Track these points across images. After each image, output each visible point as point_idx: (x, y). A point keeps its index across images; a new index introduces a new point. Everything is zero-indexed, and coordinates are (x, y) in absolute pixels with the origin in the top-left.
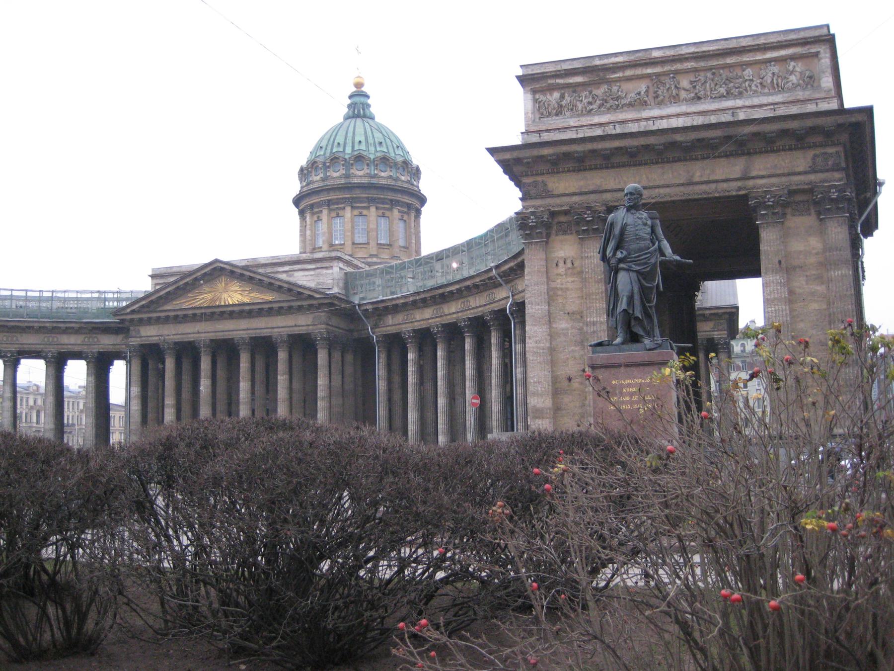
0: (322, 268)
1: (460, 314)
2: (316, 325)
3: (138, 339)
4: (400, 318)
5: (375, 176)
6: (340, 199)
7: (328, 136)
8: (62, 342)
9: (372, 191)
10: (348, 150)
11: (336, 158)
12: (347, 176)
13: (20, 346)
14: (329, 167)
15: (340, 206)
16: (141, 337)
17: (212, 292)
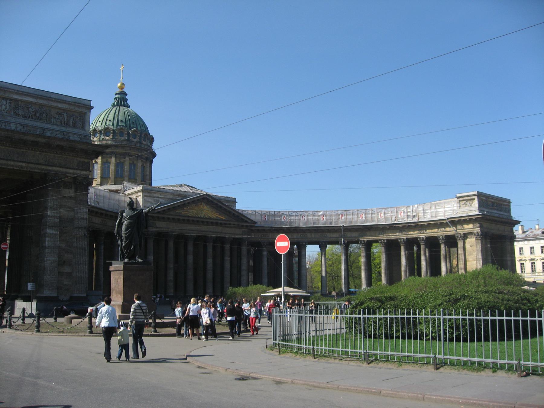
5: (149, 147)
10: (139, 128)
16: (157, 227)
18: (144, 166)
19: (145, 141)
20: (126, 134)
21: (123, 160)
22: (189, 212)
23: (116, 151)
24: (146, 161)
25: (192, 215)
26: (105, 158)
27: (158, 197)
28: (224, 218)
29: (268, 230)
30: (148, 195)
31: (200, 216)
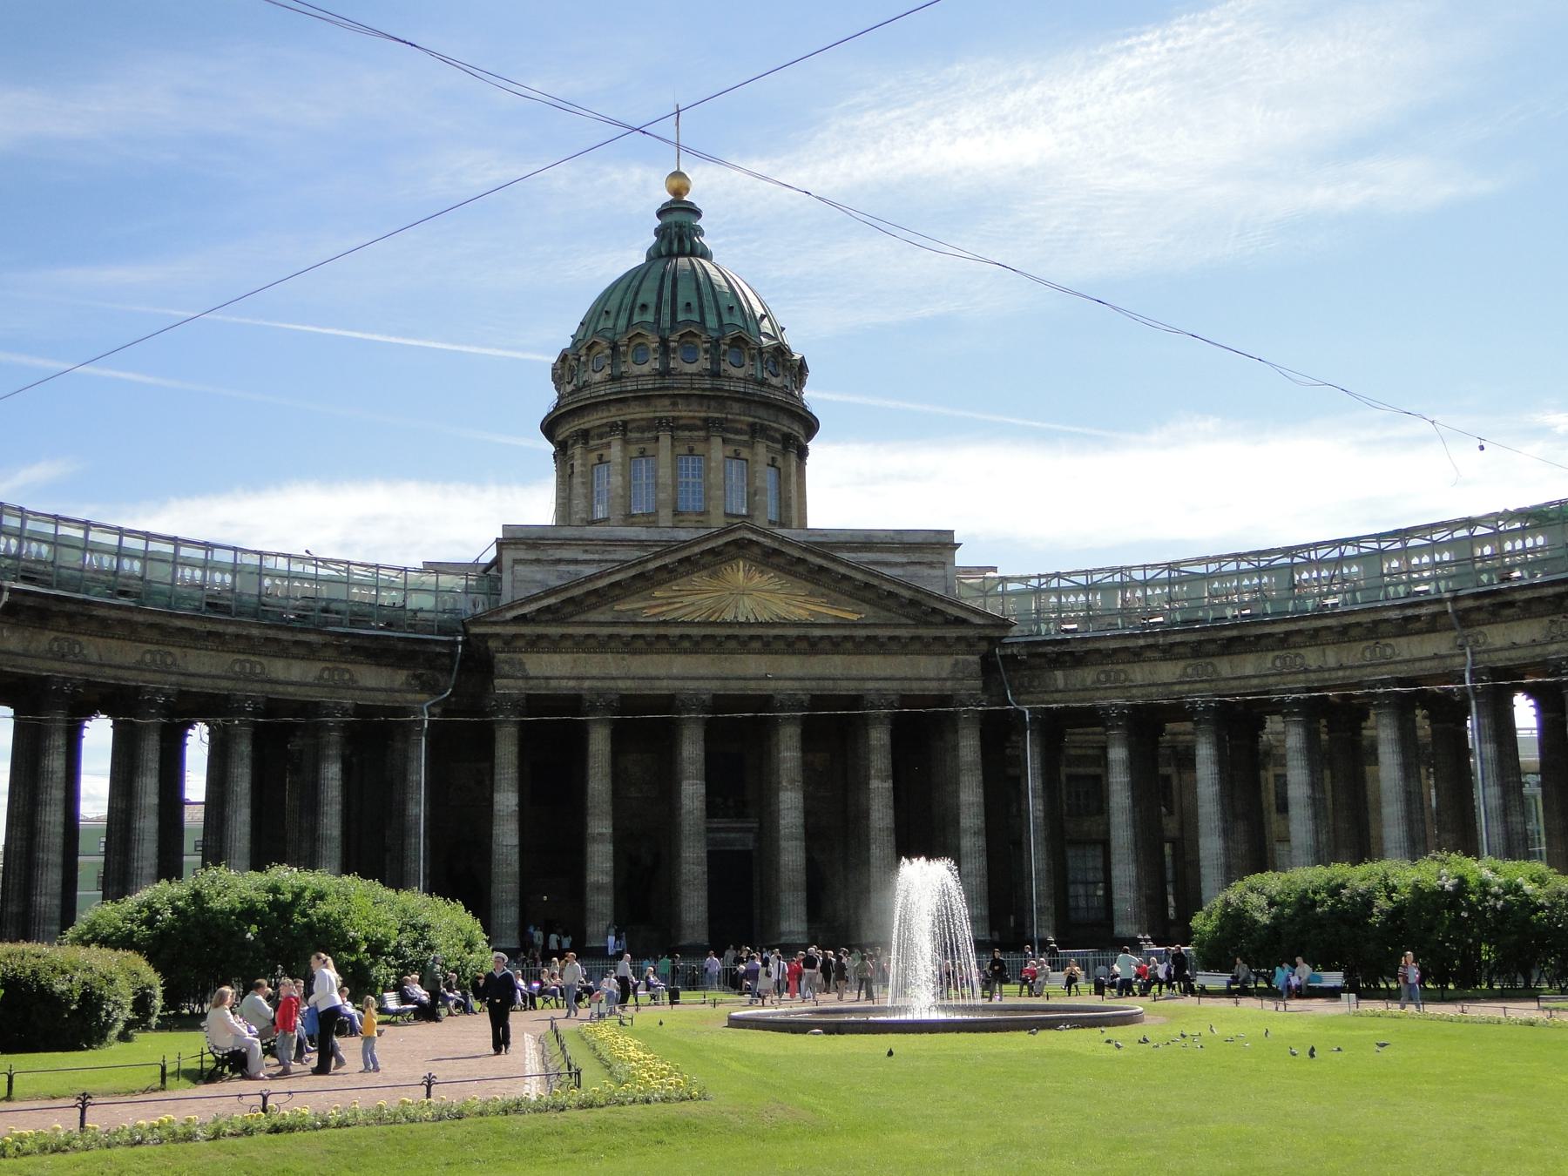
0: (920, 563)
1: (1271, 680)
2: (963, 679)
3: (521, 683)
4: (1088, 675)
5: (763, 383)
6: (700, 418)
7: (651, 285)
8: (273, 675)
9: (762, 412)
10: (712, 322)
11: (691, 333)
12: (715, 374)
13: (182, 678)
14: (674, 350)
15: (696, 433)
16: (527, 678)
17: (717, 591)
18: (747, 460)
19: (743, 366)
20: (655, 350)
21: (650, 447)
22: (679, 605)
23: (622, 418)
24: (753, 437)
25: (695, 616)
26: (596, 450)
27: (576, 562)
28: (854, 617)
29: (1115, 651)
30: (534, 557)
31: (729, 617)
